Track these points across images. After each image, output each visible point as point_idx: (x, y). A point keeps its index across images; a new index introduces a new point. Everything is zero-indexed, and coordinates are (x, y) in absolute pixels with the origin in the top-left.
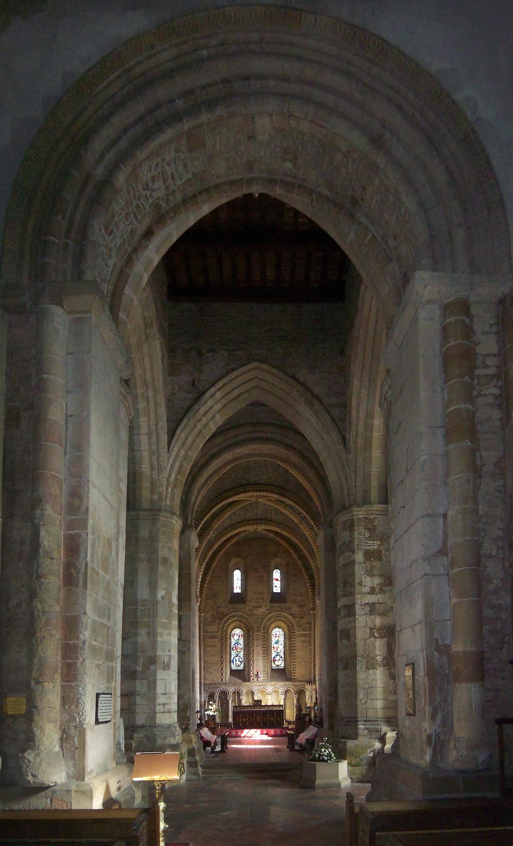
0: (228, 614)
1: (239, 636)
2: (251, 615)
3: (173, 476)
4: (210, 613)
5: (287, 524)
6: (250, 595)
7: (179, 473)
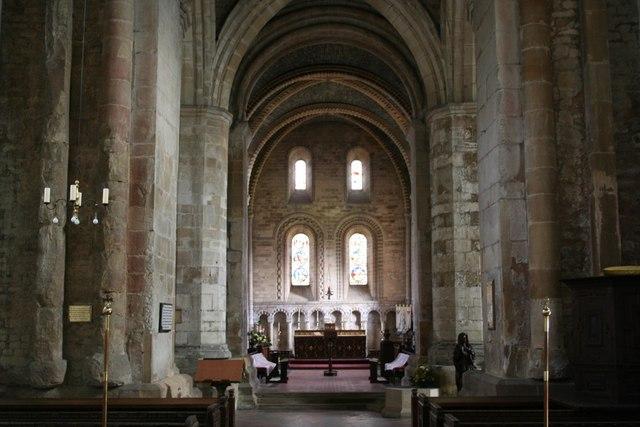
0: (287, 216)
2: (319, 218)
3: (222, 66)
5: (369, 108)
6: (319, 193)
7: (229, 63)
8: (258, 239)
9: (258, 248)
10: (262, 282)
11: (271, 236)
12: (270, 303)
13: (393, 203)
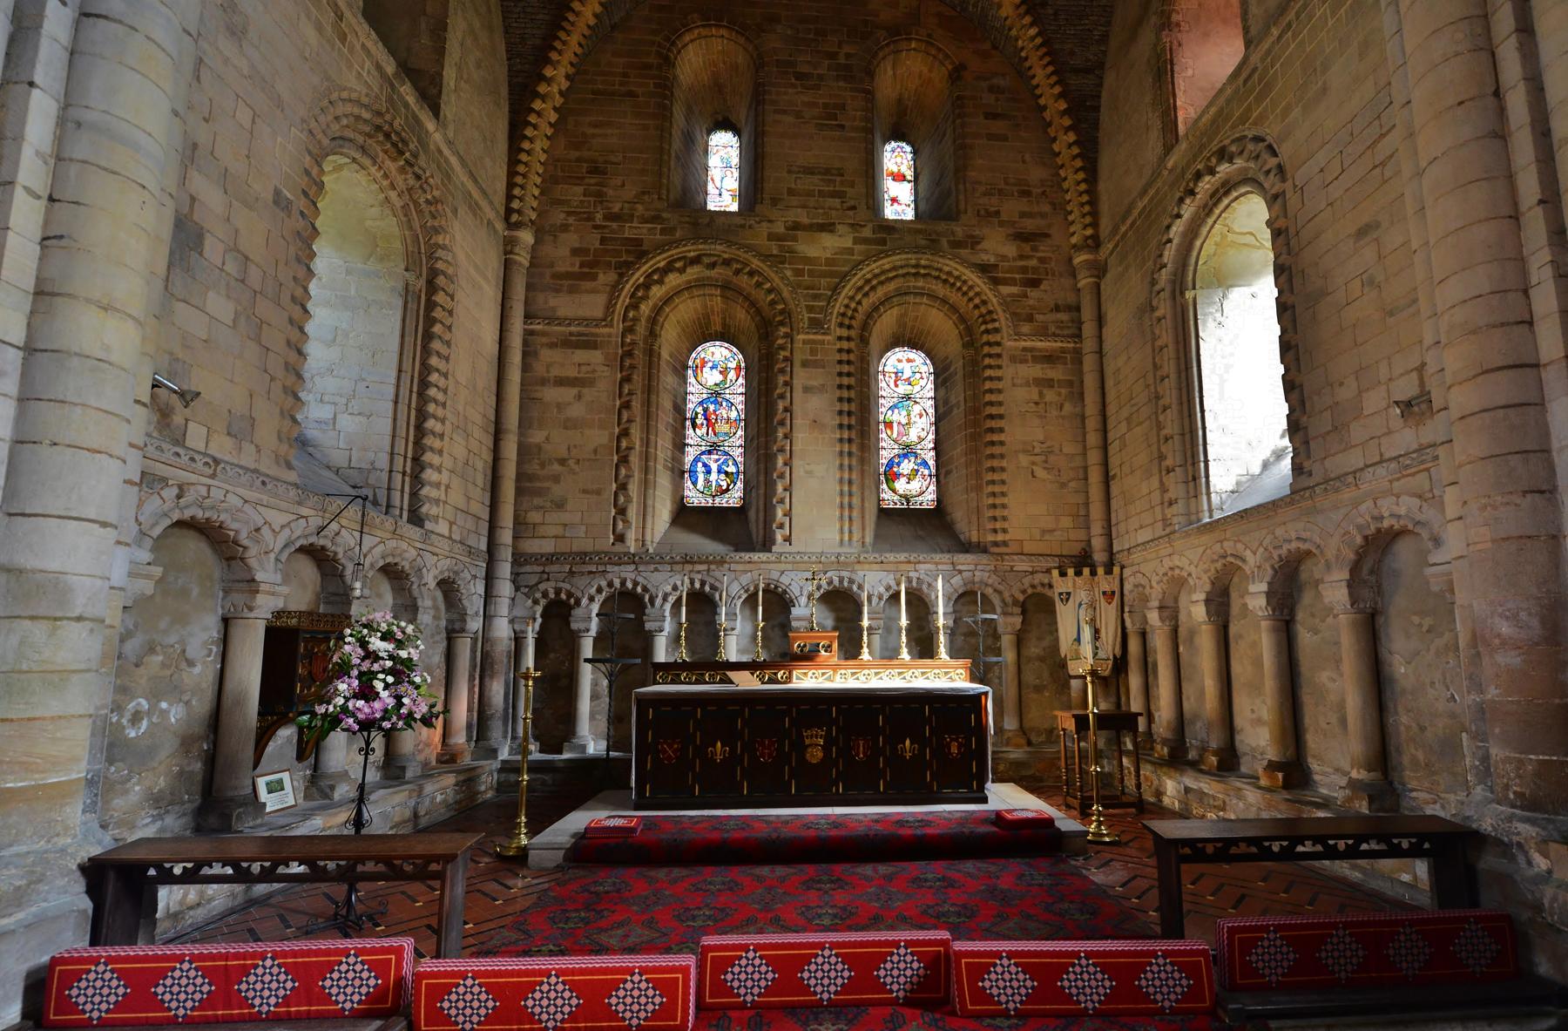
0: (661, 248)
1: (724, 372)
8: (552, 319)
9: (546, 355)
11: (598, 313)
12: (583, 557)
13: (1030, 225)
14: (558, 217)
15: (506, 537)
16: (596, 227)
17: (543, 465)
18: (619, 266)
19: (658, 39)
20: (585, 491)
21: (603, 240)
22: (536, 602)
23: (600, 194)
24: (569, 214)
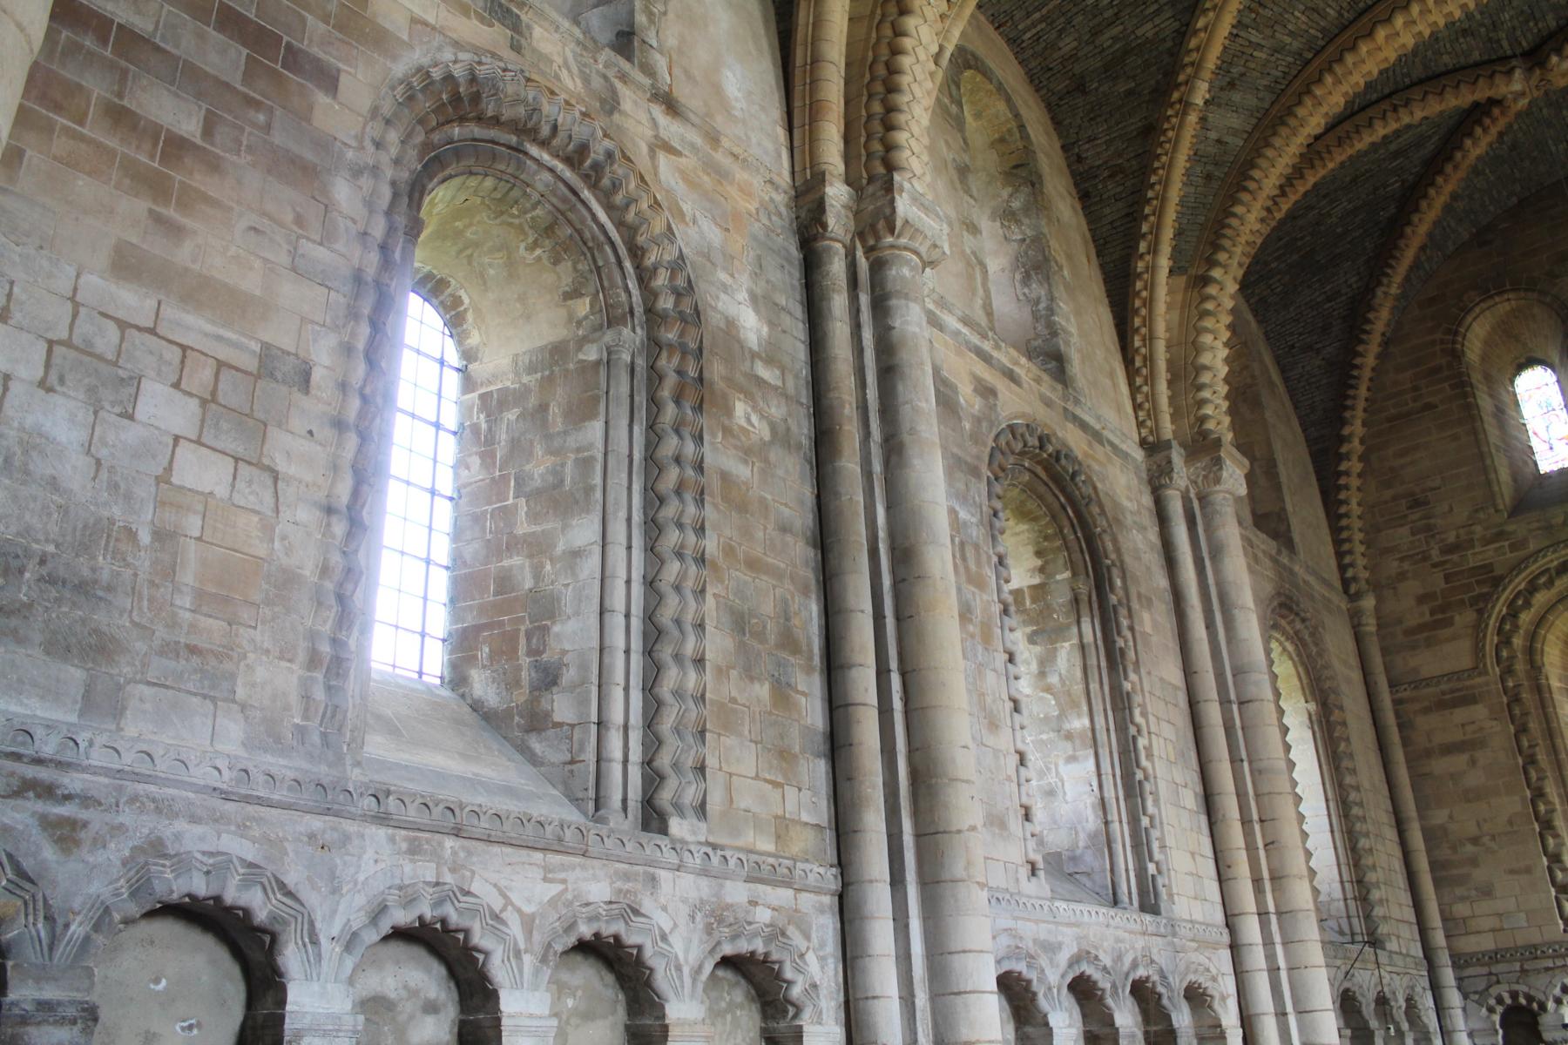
0: (1517, 567)
4: (1412, 587)
8: (1417, 684)
9: (1423, 723)
10: (1474, 862)
11: (1466, 662)
12: (1532, 952)
14: (1392, 566)
15: (1439, 938)
16: (1435, 566)
17: (1454, 848)
18: (1474, 601)
19: (1438, 336)
20: (1512, 872)
21: (1447, 578)
22: (1491, 1010)
23: (1429, 528)
24: (1402, 559)
